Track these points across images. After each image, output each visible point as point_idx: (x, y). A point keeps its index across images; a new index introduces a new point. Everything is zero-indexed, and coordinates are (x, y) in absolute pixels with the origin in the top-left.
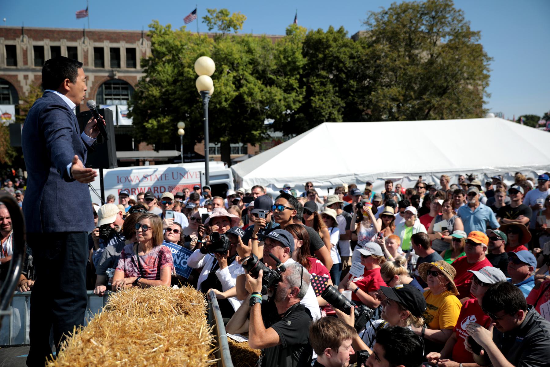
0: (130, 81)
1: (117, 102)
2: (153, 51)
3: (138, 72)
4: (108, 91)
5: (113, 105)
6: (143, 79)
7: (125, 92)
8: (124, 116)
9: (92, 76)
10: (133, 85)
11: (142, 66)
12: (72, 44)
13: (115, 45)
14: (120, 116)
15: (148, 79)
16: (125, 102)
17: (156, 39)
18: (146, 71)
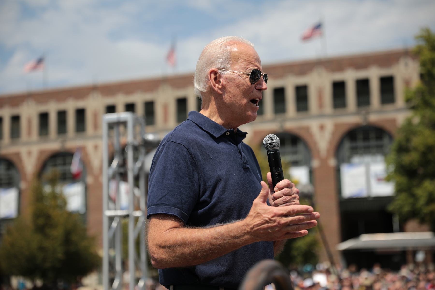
0: (388, 127)
1: (367, 159)
2: (422, 76)
3: (399, 110)
4: (354, 144)
5: (360, 164)
6: (409, 122)
7: (379, 143)
8: (379, 180)
9: (329, 124)
10: (394, 131)
11: (408, 100)
12: (301, 81)
13: (362, 74)
14: (373, 182)
15: (416, 120)
16: (379, 158)
17: (427, 55)
18: (413, 108)
